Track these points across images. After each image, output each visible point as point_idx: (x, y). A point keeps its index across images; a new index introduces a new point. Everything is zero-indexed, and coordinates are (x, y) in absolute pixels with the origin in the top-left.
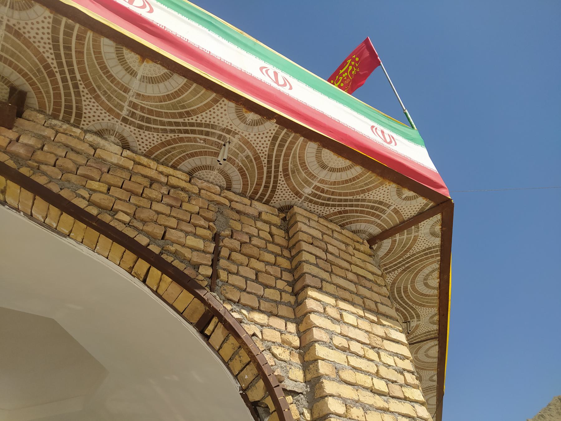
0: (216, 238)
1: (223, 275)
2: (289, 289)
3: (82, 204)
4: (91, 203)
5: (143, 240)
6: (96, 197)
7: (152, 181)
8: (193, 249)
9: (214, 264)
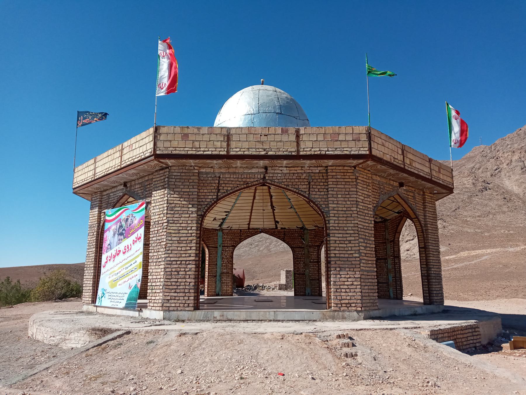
0: (309, 183)
1: (311, 193)
2: (327, 191)
3: (283, 186)
4: (285, 185)
5: (295, 190)
6: (286, 183)
7: (294, 173)
8: (305, 188)
9: (309, 191)
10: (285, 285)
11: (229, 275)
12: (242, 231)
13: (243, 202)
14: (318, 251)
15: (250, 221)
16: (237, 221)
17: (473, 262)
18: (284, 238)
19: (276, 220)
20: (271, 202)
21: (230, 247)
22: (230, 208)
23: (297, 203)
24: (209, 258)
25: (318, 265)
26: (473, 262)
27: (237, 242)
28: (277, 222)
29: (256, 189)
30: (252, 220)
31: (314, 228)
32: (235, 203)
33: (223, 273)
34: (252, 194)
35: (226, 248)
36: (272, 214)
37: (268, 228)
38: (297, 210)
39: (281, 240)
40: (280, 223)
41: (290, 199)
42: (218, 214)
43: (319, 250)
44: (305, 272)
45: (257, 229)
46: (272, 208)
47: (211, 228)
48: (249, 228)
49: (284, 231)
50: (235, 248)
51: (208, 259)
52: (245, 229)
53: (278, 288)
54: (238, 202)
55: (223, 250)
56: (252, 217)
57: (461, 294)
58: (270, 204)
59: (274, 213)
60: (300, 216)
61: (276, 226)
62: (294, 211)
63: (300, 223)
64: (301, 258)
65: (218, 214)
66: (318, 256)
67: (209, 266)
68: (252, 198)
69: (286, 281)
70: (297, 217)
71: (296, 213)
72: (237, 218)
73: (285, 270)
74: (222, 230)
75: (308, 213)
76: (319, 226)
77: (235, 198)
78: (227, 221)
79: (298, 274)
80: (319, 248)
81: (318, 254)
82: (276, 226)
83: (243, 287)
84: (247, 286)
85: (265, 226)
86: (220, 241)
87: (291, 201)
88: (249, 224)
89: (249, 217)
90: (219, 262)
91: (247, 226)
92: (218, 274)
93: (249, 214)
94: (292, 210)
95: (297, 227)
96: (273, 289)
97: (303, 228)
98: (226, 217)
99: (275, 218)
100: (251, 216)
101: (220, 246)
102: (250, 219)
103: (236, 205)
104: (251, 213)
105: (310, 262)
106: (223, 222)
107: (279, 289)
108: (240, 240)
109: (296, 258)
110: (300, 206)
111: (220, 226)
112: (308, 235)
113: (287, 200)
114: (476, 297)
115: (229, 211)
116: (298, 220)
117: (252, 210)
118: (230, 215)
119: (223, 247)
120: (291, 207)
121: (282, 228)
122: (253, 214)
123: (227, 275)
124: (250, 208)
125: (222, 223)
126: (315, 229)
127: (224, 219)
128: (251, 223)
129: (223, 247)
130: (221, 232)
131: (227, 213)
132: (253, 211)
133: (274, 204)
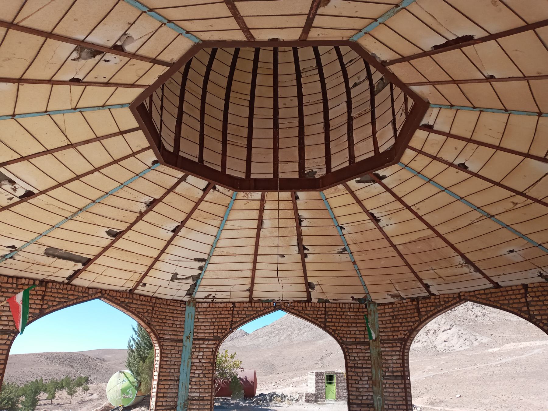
10: (315, 395)
11: (204, 405)
12: (237, 305)
13: (234, 234)
14: (403, 352)
15: (252, 284)
16: (225, 282)
17: (524, 356)
18: (326, 321)
19: (310, 280)
20: (299, 236)
21: (209, 340)
22: (207, 249)
23: (359, 237)
24: (160, 364)
25: (405, 384)
26: (524, 356)
27: (226, 329)
28: (309, 286)
29: (263, 200)
30: (256, 280)
31: (392, 300)
32: (217, 238)
33: (193, 399)
34: (256, 214)
35: (201, 342)
36: (300, 266)
37: (291, 300)
38: (357, 258)
39: (320, 326)
40: (317, 288)
41: (342, 228)
42: (181, 264)
43: (404, 349)
44: (372, 399)
45: (268, 301)
46: (300, 251)
47: (170, 298)
48: (251, 300)
49: (325, 308)
50: (220, 342)
51: (157, 366)
52: (243, 302)
53: (304, 398)
54: (224, 234)
55: (195, 348)
56: (258, 273)
57: (522, 397)
58: (295, 241)
59: (304, 263)
60: (363, 272)
61: (309, 294)
62: (349, 259)
63: (361, 289)
64: (362, 368)
65: (181, 264)
66: (403, 363)
67: (158, 384)
68: (255, 224)
69: (317, 389)
70: (354, 273)
71: (354, 263)
72: (224, 274)
73: (314, 371)
74: (195, 303)
75: (383, 263)
76: (402, 294)
77: (217, 223)
78: (204, 282)
79: (358, 405)
80: (405, 345)
81: (403, 359)
82: (309, 294)
83: (253, 395)
84: (260, 395)
85: (285, 296)
86: (189, 326)
87: (344, 232)
88: (251, 290)
89: (249, 274)
90: (184, 376)
91: (248, 294)
92: (180, 402)
93: (250, 266)
94: (345, 257)
95: (353, 298)
96: (297, 400)
97: (365, 301)
98: (200, 272)
99: (306, 277)
100: (254, 270)
101: (188, 338)
102: (253, 277)
103: (221, 243)
104: (255, 262)
105: (384, 376)
106: (195, 285)
107: (306, 401)
108: (231, 325)
109: (351, 367)
110: (366, 247)
111: (190, 293)
112: (377, 315)
113: (335, 231)
114: (542, 402)
115: (205, 257)
116: (357, 281)
117: (256, 255)
118: (210, 267)
119: (194, 339)
120: (344, 250)
121: (320, 301)
122: (258, 266)
123: (199, 405)
124: (252, 250)
125: (193, 287)
126: (392, 303)
127: (196, 278)
128: (256, 287)
129: (194, 339)
130: (194, 308)
131: (202, 264)
132: (259, 259)
133: (306, 242)
